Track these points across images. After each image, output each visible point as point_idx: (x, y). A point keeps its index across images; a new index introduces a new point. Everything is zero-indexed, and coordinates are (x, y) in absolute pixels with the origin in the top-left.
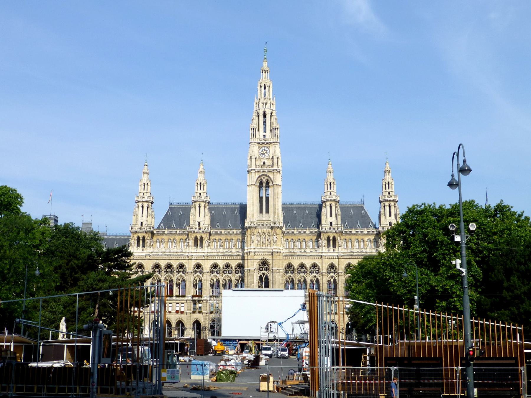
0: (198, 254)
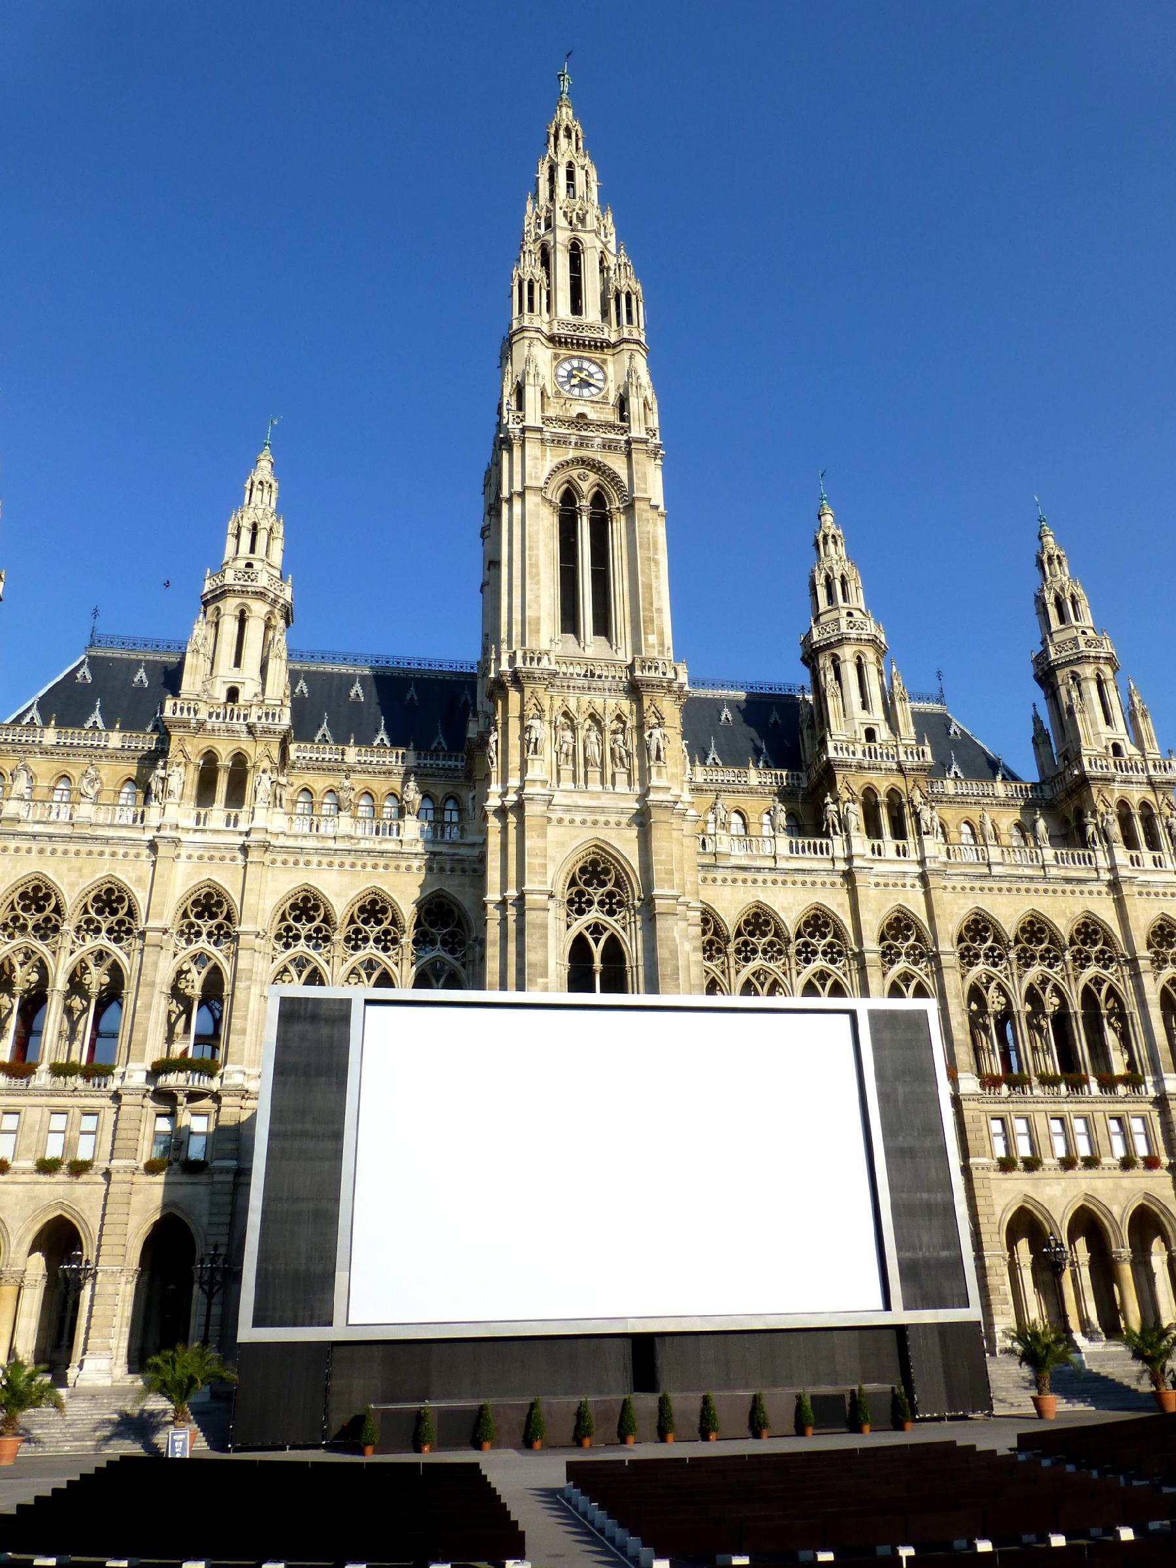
0: (209, 838)
